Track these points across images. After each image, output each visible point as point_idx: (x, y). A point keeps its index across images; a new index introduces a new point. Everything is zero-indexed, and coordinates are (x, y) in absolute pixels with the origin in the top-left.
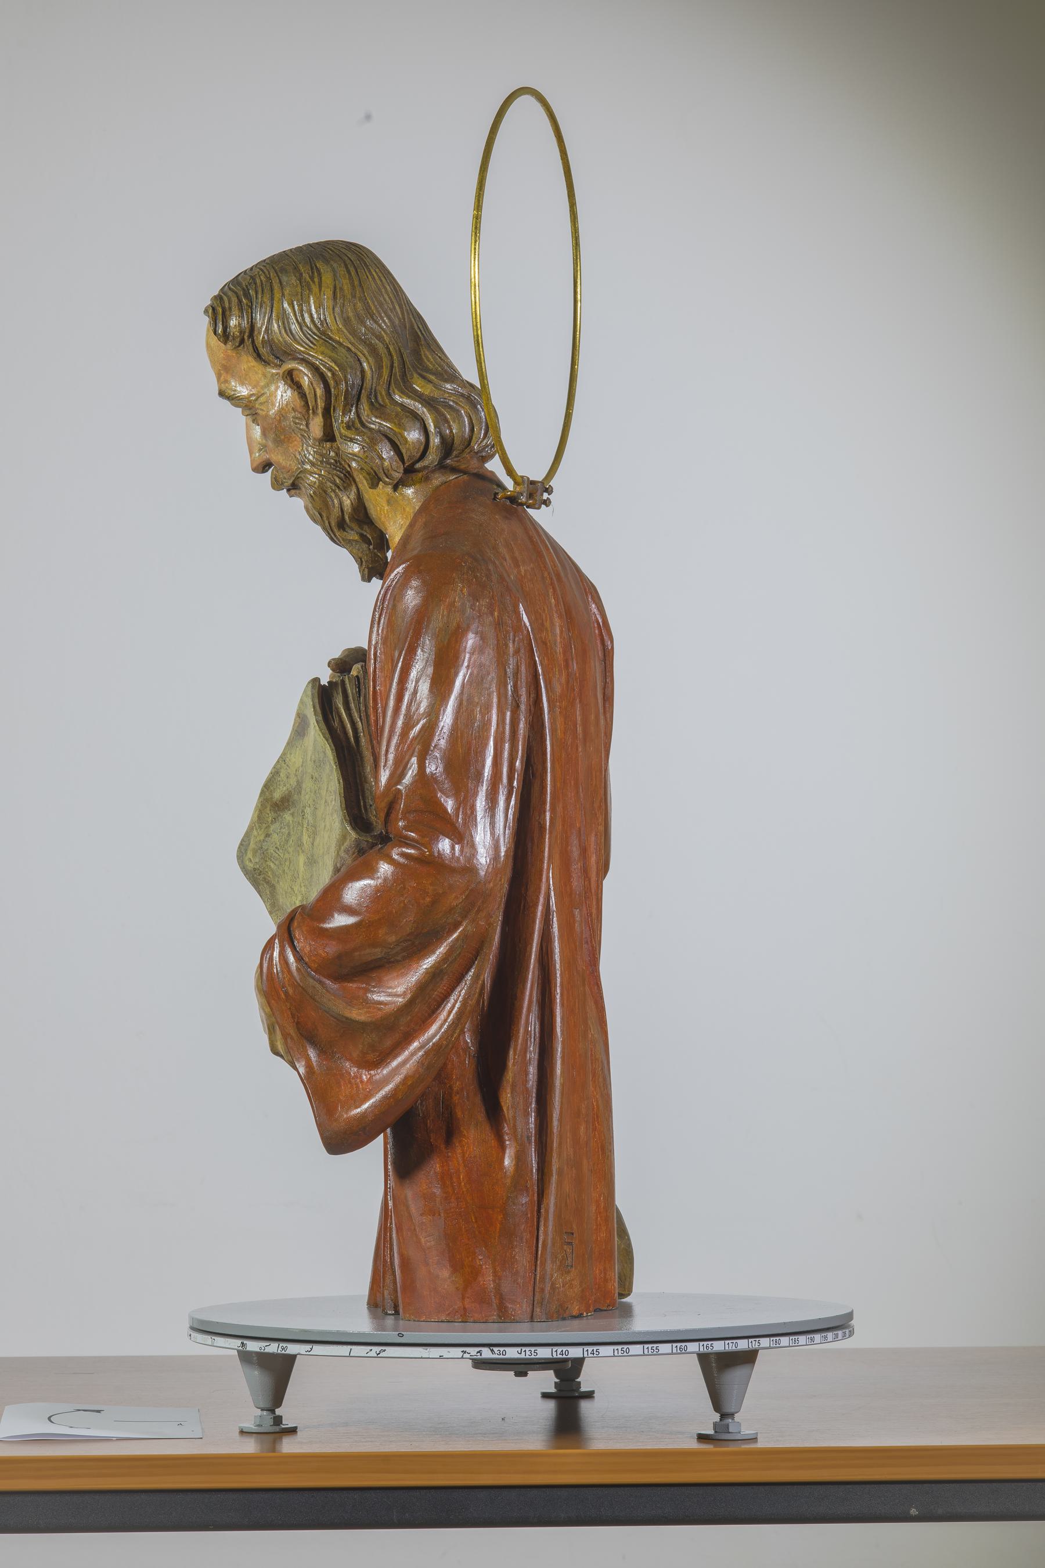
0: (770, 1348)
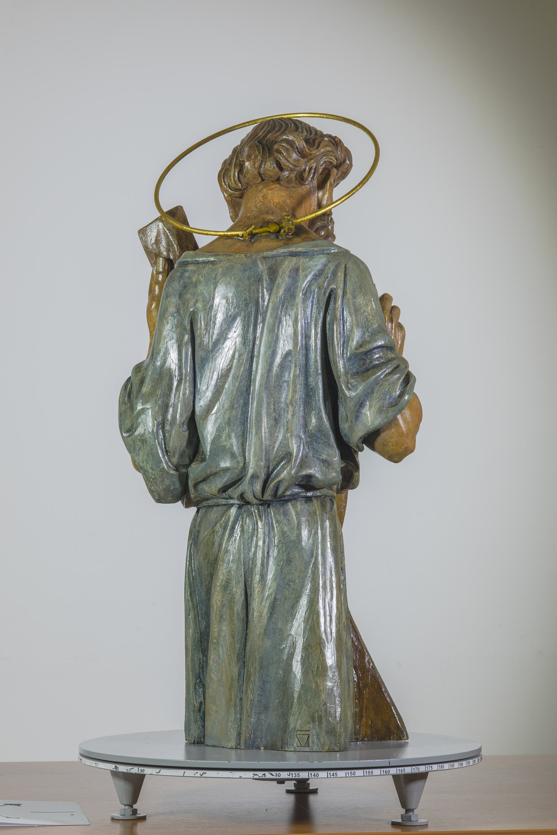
0: (438, 770)
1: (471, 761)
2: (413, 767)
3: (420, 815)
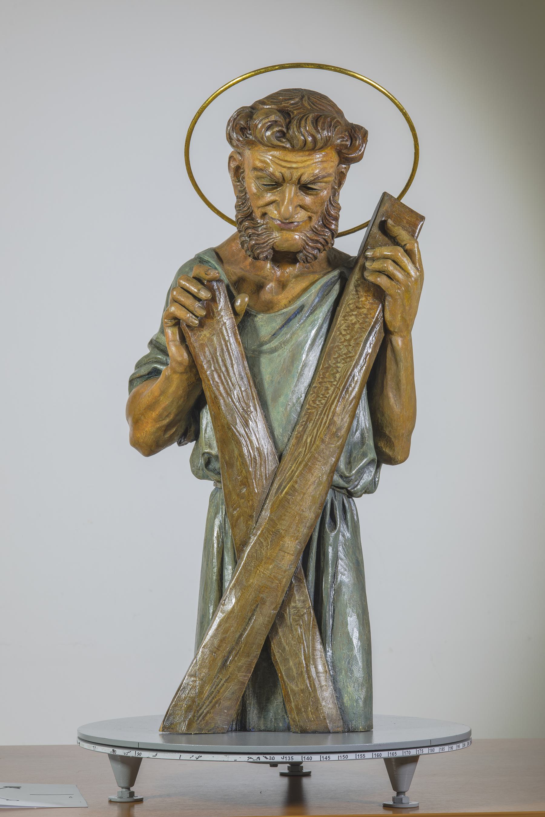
0: (428, 754)
2: (404, 751)
3: (412, 798)
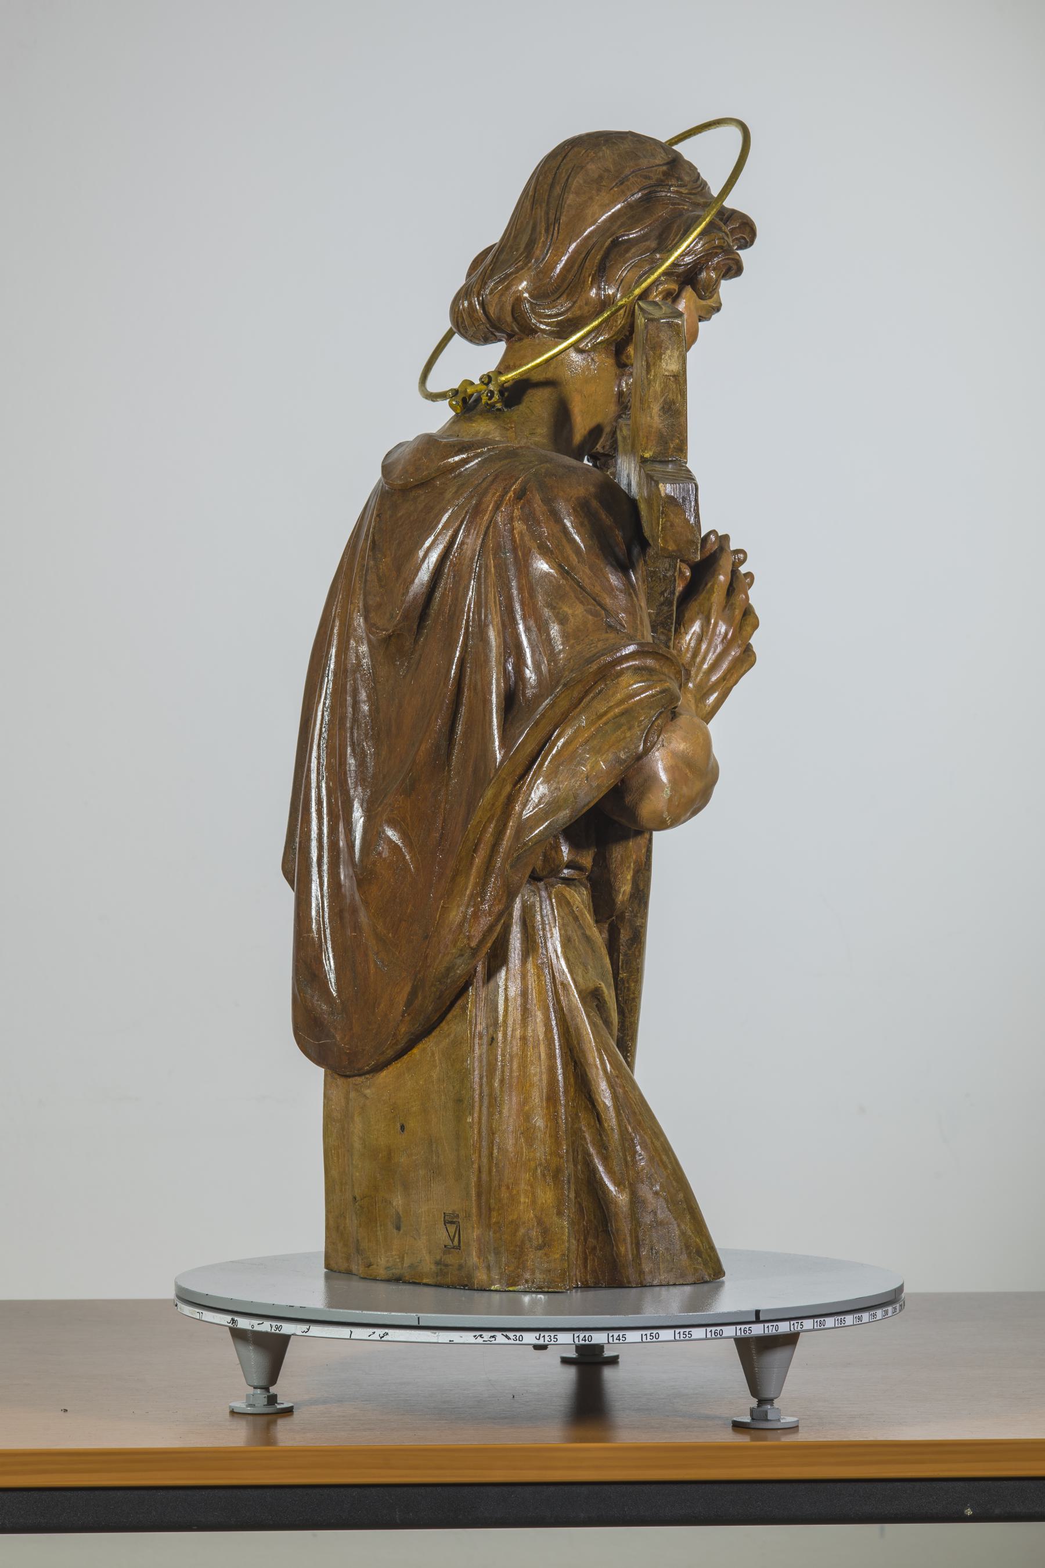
0: (814, 1330)
1: (879, 1313)
2: (766, 1325)
